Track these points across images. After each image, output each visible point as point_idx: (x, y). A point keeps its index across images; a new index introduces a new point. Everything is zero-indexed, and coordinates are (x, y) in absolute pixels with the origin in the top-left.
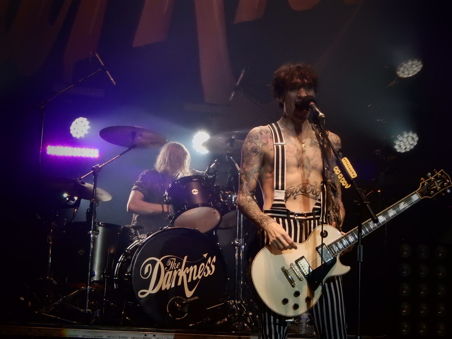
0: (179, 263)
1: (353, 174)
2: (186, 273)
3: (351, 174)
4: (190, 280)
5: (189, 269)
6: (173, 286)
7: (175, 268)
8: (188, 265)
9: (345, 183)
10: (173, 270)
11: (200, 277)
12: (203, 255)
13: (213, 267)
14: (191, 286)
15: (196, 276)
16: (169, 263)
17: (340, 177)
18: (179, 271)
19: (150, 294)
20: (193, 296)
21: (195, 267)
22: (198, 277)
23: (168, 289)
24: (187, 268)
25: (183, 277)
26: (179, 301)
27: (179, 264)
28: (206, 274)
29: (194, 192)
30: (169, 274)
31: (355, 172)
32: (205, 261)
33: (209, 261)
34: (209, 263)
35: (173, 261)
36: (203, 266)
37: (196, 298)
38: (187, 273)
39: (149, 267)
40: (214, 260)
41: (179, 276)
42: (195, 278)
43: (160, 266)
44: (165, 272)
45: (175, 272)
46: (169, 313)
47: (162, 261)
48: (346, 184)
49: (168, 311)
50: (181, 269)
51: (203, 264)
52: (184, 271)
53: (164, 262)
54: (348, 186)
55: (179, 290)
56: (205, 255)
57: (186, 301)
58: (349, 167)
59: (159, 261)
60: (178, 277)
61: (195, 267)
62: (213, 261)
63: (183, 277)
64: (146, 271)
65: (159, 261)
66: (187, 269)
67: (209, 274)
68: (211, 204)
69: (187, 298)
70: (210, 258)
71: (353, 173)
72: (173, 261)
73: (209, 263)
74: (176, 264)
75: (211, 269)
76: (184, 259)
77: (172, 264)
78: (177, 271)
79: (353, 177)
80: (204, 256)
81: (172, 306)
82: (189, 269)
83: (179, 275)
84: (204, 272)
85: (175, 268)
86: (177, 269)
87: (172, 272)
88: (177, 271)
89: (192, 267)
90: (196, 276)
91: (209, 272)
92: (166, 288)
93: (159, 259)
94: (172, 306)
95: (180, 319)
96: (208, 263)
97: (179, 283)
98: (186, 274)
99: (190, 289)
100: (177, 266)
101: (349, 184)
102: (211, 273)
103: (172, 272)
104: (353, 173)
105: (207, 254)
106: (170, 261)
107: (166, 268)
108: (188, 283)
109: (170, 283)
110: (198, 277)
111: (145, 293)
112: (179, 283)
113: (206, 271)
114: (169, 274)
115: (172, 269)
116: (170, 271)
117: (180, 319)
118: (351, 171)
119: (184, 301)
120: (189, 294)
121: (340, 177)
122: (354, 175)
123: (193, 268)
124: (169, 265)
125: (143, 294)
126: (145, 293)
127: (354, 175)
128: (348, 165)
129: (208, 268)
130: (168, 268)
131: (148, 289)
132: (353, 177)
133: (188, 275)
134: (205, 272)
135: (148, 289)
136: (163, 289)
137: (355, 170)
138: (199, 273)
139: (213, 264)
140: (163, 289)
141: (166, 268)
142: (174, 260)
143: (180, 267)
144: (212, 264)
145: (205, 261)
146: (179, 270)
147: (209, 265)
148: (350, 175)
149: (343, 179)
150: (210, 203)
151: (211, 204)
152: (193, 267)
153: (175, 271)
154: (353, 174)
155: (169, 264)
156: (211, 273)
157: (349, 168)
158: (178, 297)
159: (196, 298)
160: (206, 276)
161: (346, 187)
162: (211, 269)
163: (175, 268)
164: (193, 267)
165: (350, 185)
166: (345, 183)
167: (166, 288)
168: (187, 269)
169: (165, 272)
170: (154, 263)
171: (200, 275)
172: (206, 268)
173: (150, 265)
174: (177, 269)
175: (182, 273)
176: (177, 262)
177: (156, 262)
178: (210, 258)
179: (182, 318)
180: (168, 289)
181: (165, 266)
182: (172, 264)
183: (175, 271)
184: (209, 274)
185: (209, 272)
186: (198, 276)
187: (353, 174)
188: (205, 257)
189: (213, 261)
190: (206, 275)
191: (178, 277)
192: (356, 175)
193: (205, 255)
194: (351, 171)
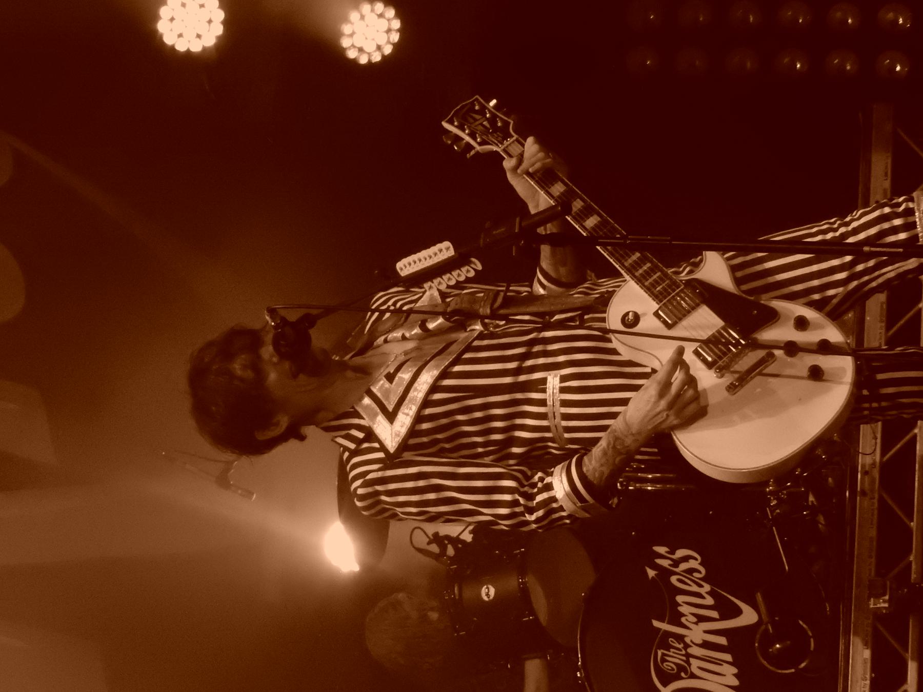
0: (671, 643)
1: (444, 250)
2: (696, 623)
3: (444, 255)
4: (714, 614)
5: (686, 616)
6: (728, 657)
7: (681, 651)
8: (676, 618)
9: (468, 271)
10: (688, 656)
11: (707, 587)
13: (680, 553)
15: (703, 597)
16: (669, 668)
17: (451, 279)
18: (691, 641)
21: (680, 599)
22: (707, 593)
24: (683, 620)
25: (706, 632)
26: (768, 641)
27: (672, 641)
28: (700, 572)
29: (487, 595)
31: (439, 246)
32: (665, 573)
33: (665, 563)
36: (680, 581)
37: (759, 597)
38: (695, 620)
40: (662, 550)
41: (703, 640)
42: (709, 601)
44: (693, 676)
45: (695, 651)
46: (795, 665)
47: (665, 685)
48: (469, 268)
49: (793, 670)
50: (685, 636)
51: (674, 579)
52: (691, 629)
54: (476, 265)
56: (651, 573)
57: (766, 624)
58: (426, 259)
60: (706, 645)
61: (680, 599)
63: (706, 632)
66: (687, 620)
67: (700, 564)
68: (518, 551)
70: (659, 561)
71: (441, 251)
73: (670, 562)
74: (672, 650)
75: (686, 559)
77: (674, 659)
78: (691, 646)
79: (451, 252)
80: (653, 577)
81: (780, 660)
82: (686, 616)
83: (701, 642)
84: (693, 576)
85: (684, 652)
86: (687, 646)
87: (692, 660)
88: (691, 646)
89: (680, 609)
91: (693, 564)
92: (735, 675)
94: (780, 660)
95: (812, 640)
96: (670, 565)
97: (722, 641)
99: (738, 612)
100: (677, 645)
101: (471, 262)
102: (696, 559)
103: (692, 660)
104: (441, 251)
106: (665, 664)
107: (683, 674)
108: (723, 617)
110: (707, 593)
112: (722, 641)
113: (691, 571)
115: (684, 658)
116: (690, 665)
117: (812, 640)
118: (436, 254)
119: (767, 630)
120: (748, 616)
121: (451, 279)
122: (448, 249)
123: (682, 604)
127: (448, 249)
128: (420, 260)
129: (683, 566)
130: (683, 671)
132: (451, 252)
133: (701, 619)
134: (696, 575)
137: (434, 245)
138: (695, 588)
139: (674, 554)
140: (735, 682)
141: (683, 674)
142: (663, 654)
143: (680, 638)
145: (665, 573)
146: (687, 640)
147: (676, 563)
148: (446, 257)
149: (455, 273)
150: (517, 554)
151: (518, 551)
152: (682, 606)
153: (690, 650)
155: (671, 667)
156: (696, 559)
157: (428, 258)
158: (757, 645)
159: (759, 597)
161: (479, 267)
162: (686, 559)
163: (684, 652)
164: (680, 605)
165: (473, 259)
166: (468, 271)
167: (735, 675)
168: (687, 620)
169: (693, 676)
171: (701, 586)
174: (687, 646)
175: (696, 633)
176: (668, 647)
178: (659, 561)
179: (811, 634)
180: (735, 671)
182: (674, 659)
183: (690, 650)
184: (700, 564)
185: (693, 564)
187: (443, 251)
188: (655, 574)
189: (667, 552)
190: (700, 572)
191: (706, 645)
193: (651, 573)
194: (436, 254)
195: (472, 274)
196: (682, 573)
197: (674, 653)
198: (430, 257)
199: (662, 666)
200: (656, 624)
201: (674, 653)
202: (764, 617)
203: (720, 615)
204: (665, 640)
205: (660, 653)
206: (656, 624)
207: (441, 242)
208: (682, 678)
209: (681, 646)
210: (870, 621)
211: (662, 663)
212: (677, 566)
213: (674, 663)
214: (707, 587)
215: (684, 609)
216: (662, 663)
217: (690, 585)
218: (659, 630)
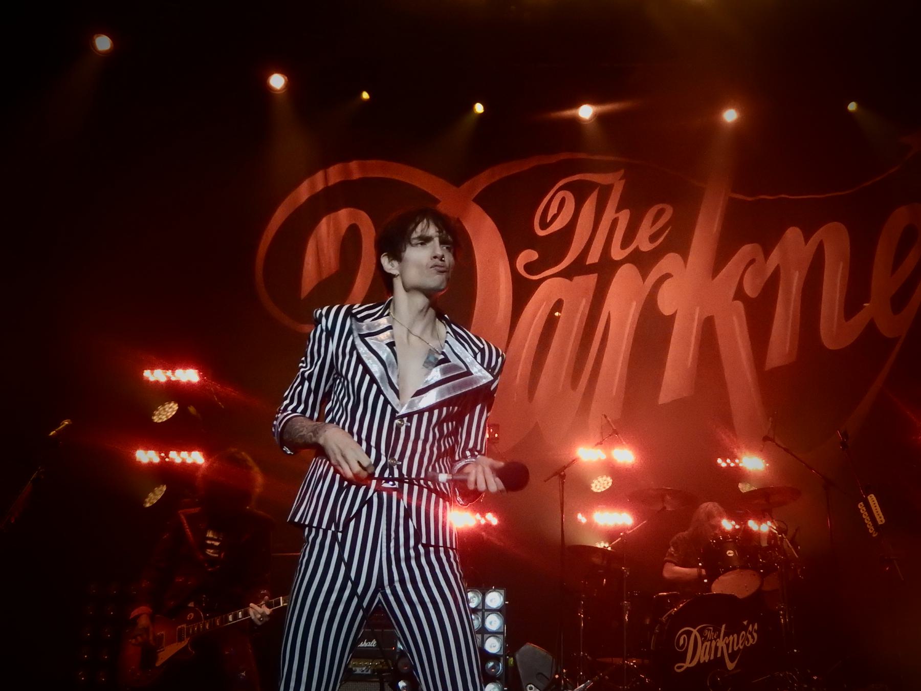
1: (880, 519)
2: (726, 643)
4: (730, 651)
5: (729, 638)
6: (712, 657)
8: (727, 634)
9: (872, 530)
10: (711, 641)
11: (741, 647)
13: (755, 635)
14: (732, 657)
19: (687, 667)
21: (735, 636)
22: (739, 648)
23: (707, 661)
24: (726, 638)
25: (722, 647)
29: (730, 553)
32: (745, 628)
33: (750, 628)
36: (743, 635)
38: (727, 642)
39: (684, 638)
40: (756, 627)
41: (718, 647)
43: (696, 637)
45: (714, 643)
47: (697, 631)
49: (708, 685)
50: (719, 639)
51: (743, 632)
52: (723, 640)
53: (701, 632)
55: (718, 662)
56: (745, 623)
59: (695, 632)
60: (717, 648)
61: (735, 636)
63: (722, 647)
64: (682, 642)
65: (695, 632)
71: (880, 517)
75: (753, 637)
77: (709, 634)
79: (880, 523)
80: (743, 623)
83: (718, 645)
86: (715, 639)
87: (710, 642)
89: (731, 636)
91: (751, 640)
92: (705, 661)
93: (695, 629)
97: (719, 655)
98: (725, 645)
99: (732, 661)
100: (715, 635)
102: (753, 641)
103: (710, 642)
111: (682, 667)
112: (719, 655)
116: (708, 641)
118: (878, 515)
120: (730, 666)
122: (881, 521)
125: (679, 668)
126: (682, 667)
127: (881, 521)
129: (750, 636)
130: (705, 638)
131: (684, 662)
132: (880, 523)
133: (728, 645)
134: (746, 642)
135: (684, 662)
136: (702, 662)
137: (883, 515)
138: (740, 642)
139: (755, 632)
140: (702, 662)
142: (711, 630)
143: (719, 637)
144: (753, 632)
145: (745, 628)
146: (718, 640)
147: (751, 633)
148: (878, 520)
153: (714, 641)
154: (880, 519)
159: (739, 671)
160: (749, 645)
162: (753, 637)
167: (705, 661)
169: (703, 643)
170: (689, 633)
171: (742, 645)
173: (685, 636)
174: (715, 639)
175: (721, 643)
177: (691, 632)
180: (707, 661)
181: (701, 636)
182: (709, 634)
183: (714, 641)
185: (751, 640)
186: (740, 645)
187: (881, 519)
190: (748, 644)
191: (717, 648)
192: (884, 521)
193: (745, 623)
194: (878, 515)
195: (870, 531)
198: (877, 512)
200: (724, 626)
204: (717, 630)
205: (711, 628)
206: (724, 626)
207: (884, 518)
208: (701, 638)
209: (715, 637)
212: (749, 634)
213: (707, 635)
214: (741, 647)
215: (731, 638)
217: (742, 639)
218: (721, 627)
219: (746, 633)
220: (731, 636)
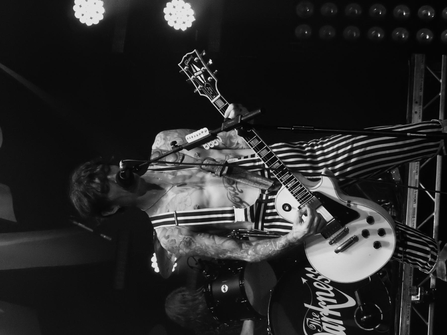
0: (313, 315)
2: (326, 305)
4: (335, 301)
5: (321, 302)
6: (341, 322)
7: (318, 319)
8: (316, 303)
10: (321, 321)
11: (331, 288)
12: (304, 282)
15: (329, 293)
16: (312, 327)
18: (323, 314)
20: (355, 298)
21: (318, 293)
22: (331, 291)
24: (319, 304)
25: (330, 310)
26: (360, 315)
27: (314, 314)
28: (328, 281)
29: (224, 289)
30: (327, 327)
32: (311, 281)
34: (314, 276)
35: (311, 322)
36: (318, 284)
38: (325, 304)
42: (332, 295)
45: (324, 319)
46: (374, 327)
49: (372, 329)
50: (320, 312)
51: (315, 284)
52: (322, 308)
56: (304, 281)
57: (360, 306)
60: (330, 316)
61: (318, 293)
62: (312, 271)
63: (330, 310)
66: (321, 304)
68: (240, 268)
69: (357, 305)
70: (308, 275)
72: (311, 322)
73: (314, 276)
74: (314, 318)
76: (308, 308)
77: (314, 323)
78: (323, 317)
80: (305, 283)
81: (367, 324)
82: (321, 302)
83: (327, 315)
85: (319, 319)
86: (321, 316)
87: (323, 323)
88: (323, 317)
89: (318, 298)
90: (329, 293)
92: (344, 331)
94: (367, 324)
95: (382, 315)
96: (313, 277)
97: (338, 314)
98: (327, 306)
99: (346, 300)
100: (316, 316)
103: (323, 323)
105: (303, 278)
106: (310, 325)
107: (319, 330)
108: (339, 303)
109: (338, 326)
110: (331, 291)
112: (338, 314)
114: (327, 327)
115: (320, 322)
116: (322, 326)
117: (382, 315)
119: (360, 309)
120: (351, 302)
124: (314, 326)
133: (328, 303)
134: (326, 282)
138: (325, 288)
141: (319, 330)
142: (309, 320)
143: (318, 312)
145: (311, 281)
146: (321, 313)
150: (240, 270)
152: (318, 297)
153: (322, 319)
155: (313, 327)
158: (355, 316)
163: (319, 319)
164: (318, 297)
167: (344, 331)
168: (321, 304)
171: (328, 287)
172: (320, 280)
174: (321, 316)
175: (325, 310)
176: (312, 317)
178: (308, 275)
179: (381, 312)
180: (344, 329)
182: (314, 323)
183: (322, 319)
188: (306, 281)
189: (312, 271)
190: (328, 281)
191: (330, 316)
193: (304, 281)
196: (319, 281)
197: (314, 319)
198: (200, 134)
199: (308, 325)
200: (306, 305)
201: (314, 319)
202: (359, 303)
203: (337, 301)
204: (310, 313)
205: (308, 319)
206: (306, 305)
208: (318, 332)
209: (318, 316)
210: (410, 307)
211: (309, 325)
215: (320, 298)
216: (309, 325)
217: (323, 287)
219: (316, 281)
220: (318, 298)
